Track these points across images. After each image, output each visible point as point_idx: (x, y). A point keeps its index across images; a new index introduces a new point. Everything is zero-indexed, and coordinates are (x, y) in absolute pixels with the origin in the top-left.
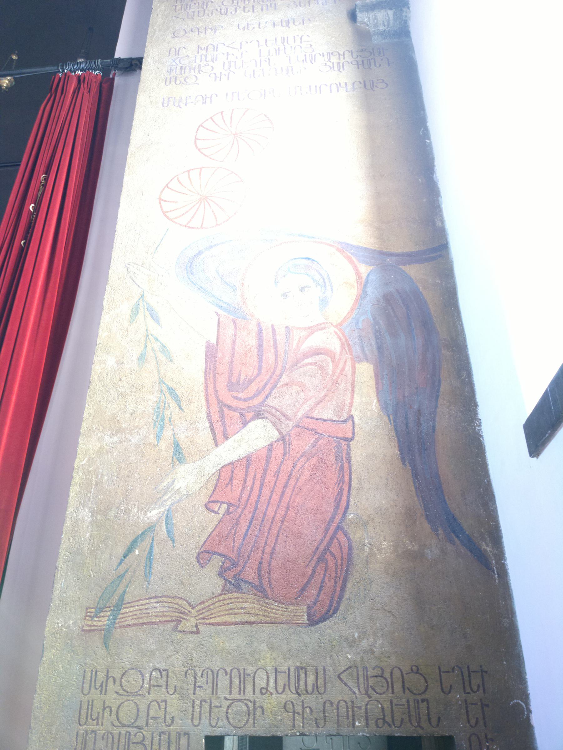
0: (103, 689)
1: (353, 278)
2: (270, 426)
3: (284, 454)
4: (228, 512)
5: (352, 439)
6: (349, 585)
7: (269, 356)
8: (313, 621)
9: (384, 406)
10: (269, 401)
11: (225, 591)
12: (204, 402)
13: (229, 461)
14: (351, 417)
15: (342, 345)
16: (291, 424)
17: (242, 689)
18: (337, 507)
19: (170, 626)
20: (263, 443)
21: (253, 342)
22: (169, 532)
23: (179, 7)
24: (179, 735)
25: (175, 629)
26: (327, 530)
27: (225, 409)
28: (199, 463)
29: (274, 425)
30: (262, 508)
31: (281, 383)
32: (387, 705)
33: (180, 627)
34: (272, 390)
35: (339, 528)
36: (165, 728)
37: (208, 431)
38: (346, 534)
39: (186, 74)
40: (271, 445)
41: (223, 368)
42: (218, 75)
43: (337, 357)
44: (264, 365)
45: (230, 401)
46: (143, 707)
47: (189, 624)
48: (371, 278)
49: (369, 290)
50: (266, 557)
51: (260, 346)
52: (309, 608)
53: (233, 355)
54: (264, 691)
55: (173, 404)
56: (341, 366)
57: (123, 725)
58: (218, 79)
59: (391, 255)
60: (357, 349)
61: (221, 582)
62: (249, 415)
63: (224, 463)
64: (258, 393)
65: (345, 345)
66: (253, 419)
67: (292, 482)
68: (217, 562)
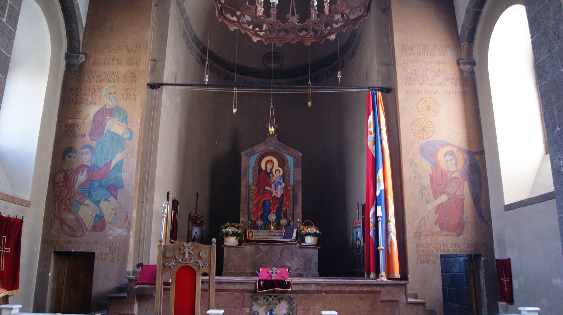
0: (420, 247)
1: (463, 158)
2: (446, 196)
3: (450, 203)
4: (439, 215)
5: (464, 200)
6: (464, 229)
7: (445, 178)
8: (458, 236)
9: (470, 193)
10: (446, 190)
11: (441, 230)
12: (431, 189)
13: (438, 204)
14: (464, 195)
15: (461, 176)
16: (451, 196)
17: (446, 247)
18: (461, 213)
19: (431, 236)
20: (445, 200)
21: (441, 174)
22: (428, 218)
23: (403, 49)
24: (435, 254)
25: (432, 236)
26: (460, 218)
27: (436, 192)
28: (432, 204)
29: (447, 195)
30: (446, 214)
31: (448, 186)
32: (471, 249)
33: (433, 236)
34: (446, 187)
35: (462, 219)
36: (432, 253)
37: (433, 197)
38: (463, 220)
39: (411, 81)
40: (447, 200)
41: (434, 181)
42: (421, 83)
43: (460, 180)
44: (444, 181)
45: (437, 190)
46: (428, 250)
47: (435, 236)
48: (467, 159)
49: (467, 162)
50: (448, 224)
51: (442, 175)
52: (457, 233)
53: (436, 178)
54: (450, 247)
55: (424, 190)
56: (461, 182)
57: (425, 253)
58: (421, 84)
59: (471, 152)
60: (464, 177)
61: (440, 228)
62: (442, 193)
63: (437, 204)
64: (443, 188)
65: (462, 177)
66: (442, 194)
67: (452, 209)
68: (438, 225)
